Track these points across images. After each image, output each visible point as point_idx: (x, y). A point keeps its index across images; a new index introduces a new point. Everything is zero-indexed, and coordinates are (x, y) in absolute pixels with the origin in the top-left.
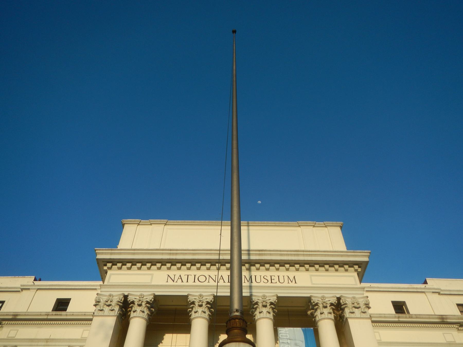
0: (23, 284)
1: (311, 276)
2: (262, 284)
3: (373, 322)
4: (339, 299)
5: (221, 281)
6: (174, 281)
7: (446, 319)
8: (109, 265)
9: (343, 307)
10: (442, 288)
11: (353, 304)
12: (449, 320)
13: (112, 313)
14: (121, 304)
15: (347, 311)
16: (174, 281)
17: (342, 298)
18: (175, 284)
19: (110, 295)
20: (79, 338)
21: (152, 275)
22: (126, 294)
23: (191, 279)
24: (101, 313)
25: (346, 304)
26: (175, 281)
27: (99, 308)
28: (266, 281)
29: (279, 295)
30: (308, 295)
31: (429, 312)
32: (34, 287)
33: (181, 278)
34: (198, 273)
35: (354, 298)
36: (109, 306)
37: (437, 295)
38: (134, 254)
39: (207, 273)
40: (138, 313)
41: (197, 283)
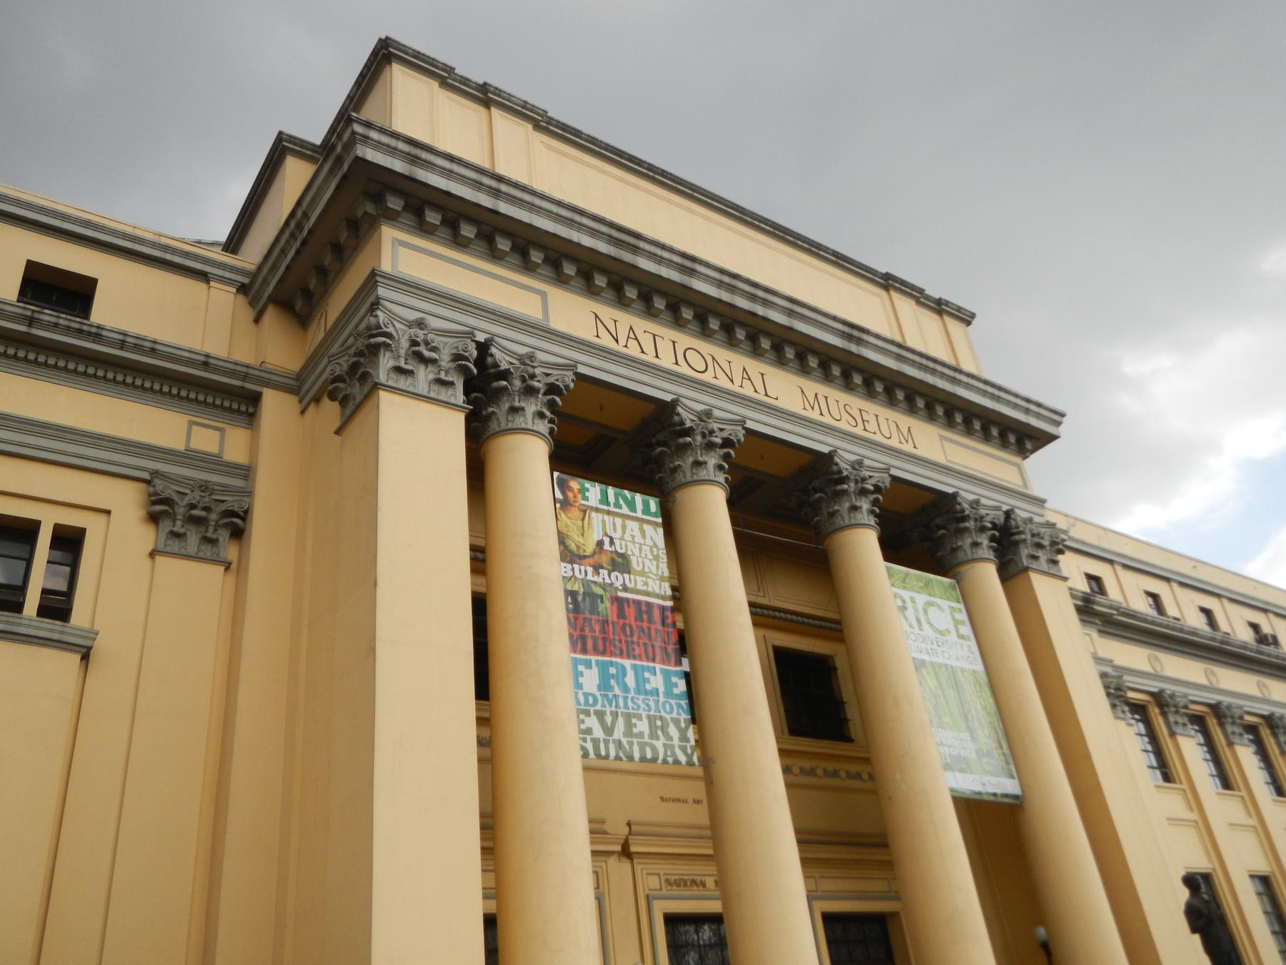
1: (942, 437)
2: (843, 425)
4: (1008, 514)
8: (395, 203)
9: (1017, 537)
13: (444, 394)
15: (1025, 552)
18: (619, 348)
19: (420, 324)
20: (180, 446)
21: (543, 295)
22: (481, 337)
23: (665, 348)
24: (403, 383)
26: (622, 341)
27: (392, 363)
39: (706, 348)
41: (684, 369)
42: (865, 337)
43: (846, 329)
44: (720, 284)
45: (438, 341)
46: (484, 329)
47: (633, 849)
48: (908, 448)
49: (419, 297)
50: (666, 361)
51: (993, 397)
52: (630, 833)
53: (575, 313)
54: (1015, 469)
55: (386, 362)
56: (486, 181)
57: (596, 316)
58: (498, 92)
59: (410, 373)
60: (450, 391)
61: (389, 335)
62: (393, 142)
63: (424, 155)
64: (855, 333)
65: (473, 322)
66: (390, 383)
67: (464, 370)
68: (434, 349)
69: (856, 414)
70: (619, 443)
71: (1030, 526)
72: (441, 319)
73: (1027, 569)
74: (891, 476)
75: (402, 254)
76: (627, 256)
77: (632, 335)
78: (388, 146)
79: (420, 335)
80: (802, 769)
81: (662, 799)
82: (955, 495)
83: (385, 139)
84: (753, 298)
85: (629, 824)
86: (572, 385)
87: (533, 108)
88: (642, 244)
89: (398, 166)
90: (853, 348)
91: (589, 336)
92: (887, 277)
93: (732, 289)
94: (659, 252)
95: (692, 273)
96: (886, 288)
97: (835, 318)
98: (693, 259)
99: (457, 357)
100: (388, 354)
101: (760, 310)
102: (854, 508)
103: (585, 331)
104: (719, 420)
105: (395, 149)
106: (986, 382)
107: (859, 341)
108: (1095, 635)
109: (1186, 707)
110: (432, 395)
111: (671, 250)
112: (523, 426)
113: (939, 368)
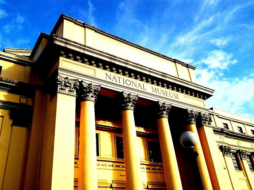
3: (214, 130)
5: (140, 87)
6: (111, 79)
7: (224, 130)
12: (224, 131)
14: (79, 88)
16: (111, 79)
19: (67, 78)
21: (95, 70)
22: (80, 80)
24: (62, 91)
26: (112, 79)
27: (60, 87)
28: (164, 94)
33: (115, 79)
34: (126, 78)
36: (68, 86)
37: (217, 117)
41: (126, 85)
44: (134, 66)
45: (70, 82)
46: (80, 78)
47: (113, 186)
48: (176, 99)
49: (67, 72)
50: (121, 83)
52: (112, 183)
53: (101, 74)
54: (203, 103)
55: (59, 87)
56: (82, 47)
57: (106, 74)
59: (64, 89)
60: (73, 93)
61: (60, 81)
62: (62, 40)
63: (69, 42)
64: (165, 75)
66: (60, 92)
67: (76, 88)
68: (70, 84)
69: (165, 93)
71: (205, 116)
72: (71, 77)
73: (203, 125)
74: (171, 106)
75: (64, 63)
77: (114, 78)
78: (61, 41)
80: (152, 169)
81: (120, 175)
82: (187, 109)
85: (112, 181)
86: (100, 90)
88: (116, 59)
89: (63, 45)
90: (164, 78)
91: (104, 79)
92: (175, 60)
93: (136, 67)
99: (74, 85)
100: (60, 85)
102: (163, 113)
103: (103, 77)
105: (62, 41)
107: (165, 77)
108: (224, 137)
109: (245, 153)
110: (69, 94)
111: (123, 60)
112: (89, 99)
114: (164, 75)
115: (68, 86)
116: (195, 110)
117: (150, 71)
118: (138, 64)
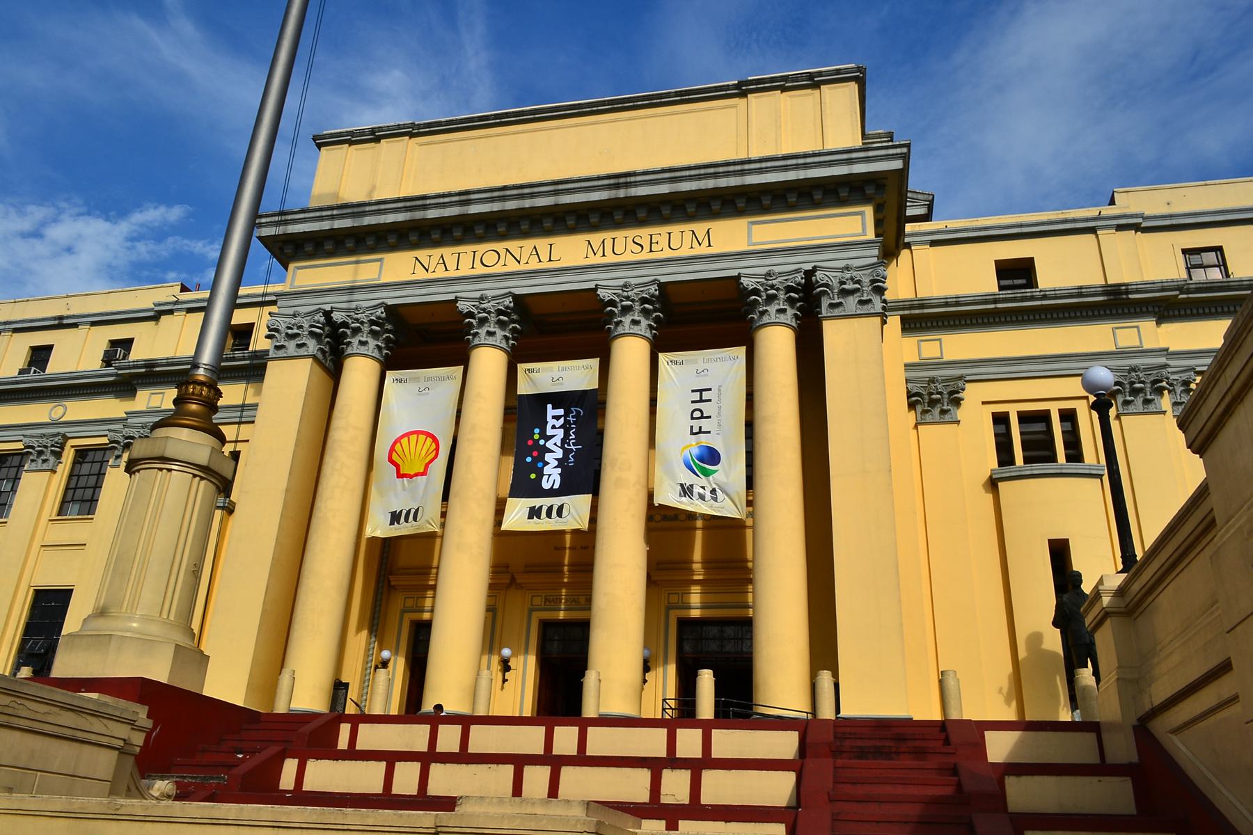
0: (157, 300)
4: (809, 274)
10: (1147, 213)
11: (842, 283)
13: (302, 351)
15: (825, 302)
17: (818, 273)
19: (294, 316)
22: (328, 308)
23: (466, 261)
25: (826, 285)
29: (663, 279)
30: (735, 273)
31: (1093, 278)
32: (179, 306)
34: (481, 248)
35: (847, 268)
38: (332, 217)
39: (500, 246)
40: (355, 347)
41: (479, 270)
42: (633, 179)
43: (612, 181)
44: (492, 200)
46: (326, 303)
51: (797, 167)
58: (381, 129)
64: (622, 180)
65: (328, 299)
67: (312, 334)
68: (300, 327)
70: (424, 338)
76: (419, 215)
79: (293, 321)
82: (739, 276)
83: (268, 220)
84: (521, 197)
87: (404, 126)
88: (428, 202)
90: (622, 193)
93: (503, 199)
94: (441, 200)
95: (468, 202)
96: (743, 94)
97: (599, 178)
98: (467, 193)
101: (527, 203)
104: (494, 298)
106: (785, 158)
107: (627, 185)
111: (450, 195)
113: (721, 169)
114: (621, 180)
115: (297, 335)
116: (789, 268)
117: (557, 193)
118: (505, 188)
